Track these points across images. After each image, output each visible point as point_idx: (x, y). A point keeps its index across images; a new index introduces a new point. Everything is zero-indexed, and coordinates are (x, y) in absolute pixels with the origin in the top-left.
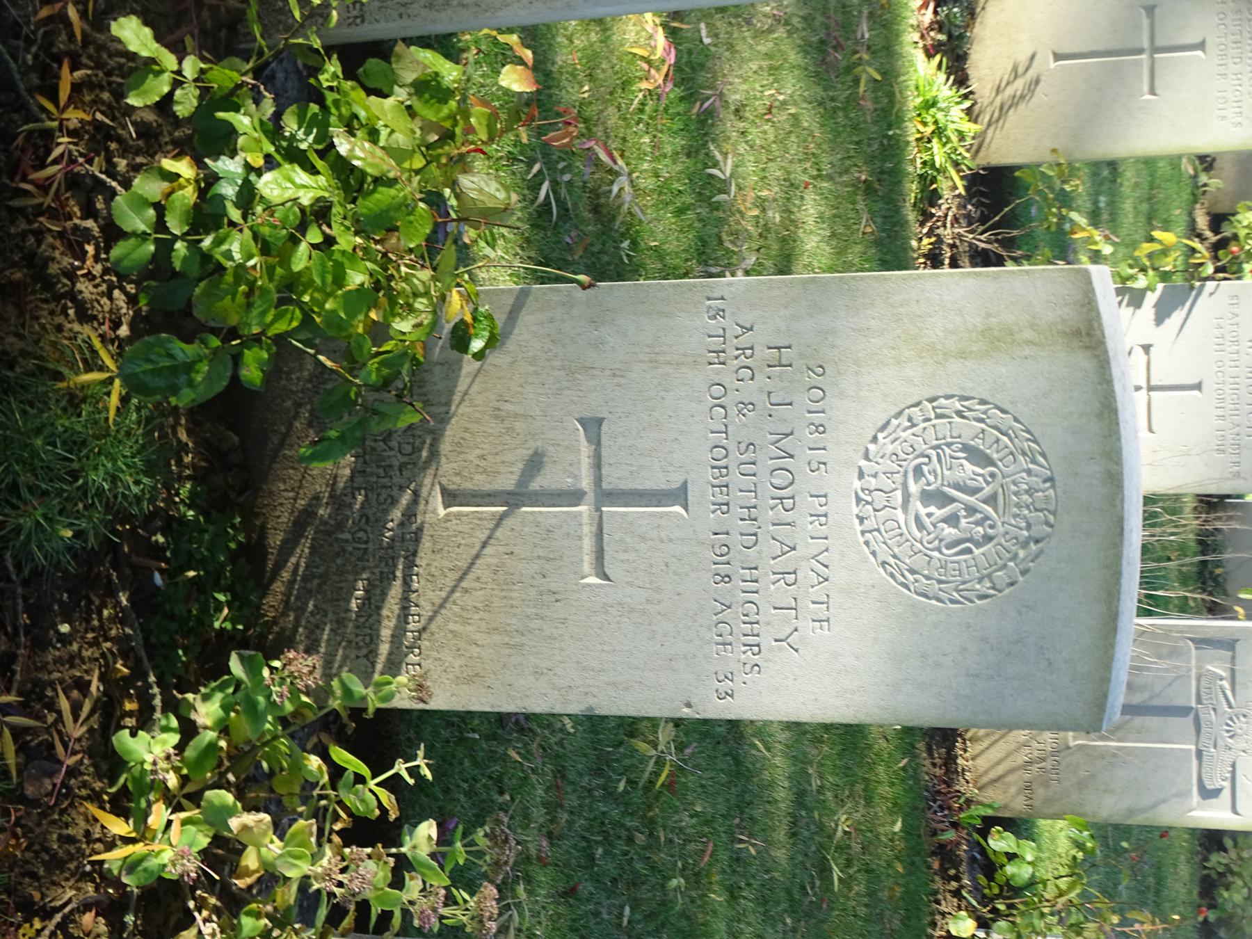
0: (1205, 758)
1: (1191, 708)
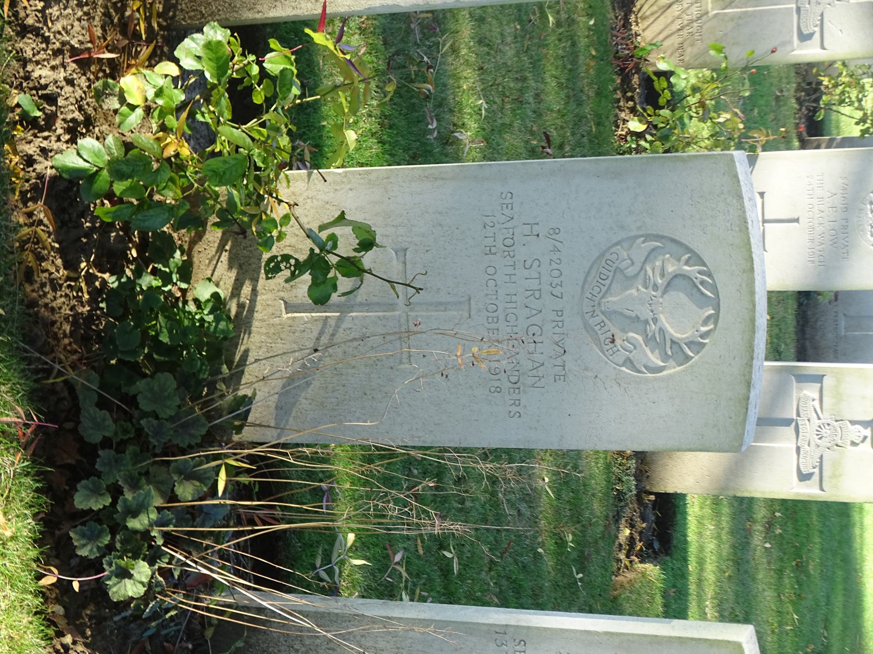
0: (802, 452)
1: (793, 420)
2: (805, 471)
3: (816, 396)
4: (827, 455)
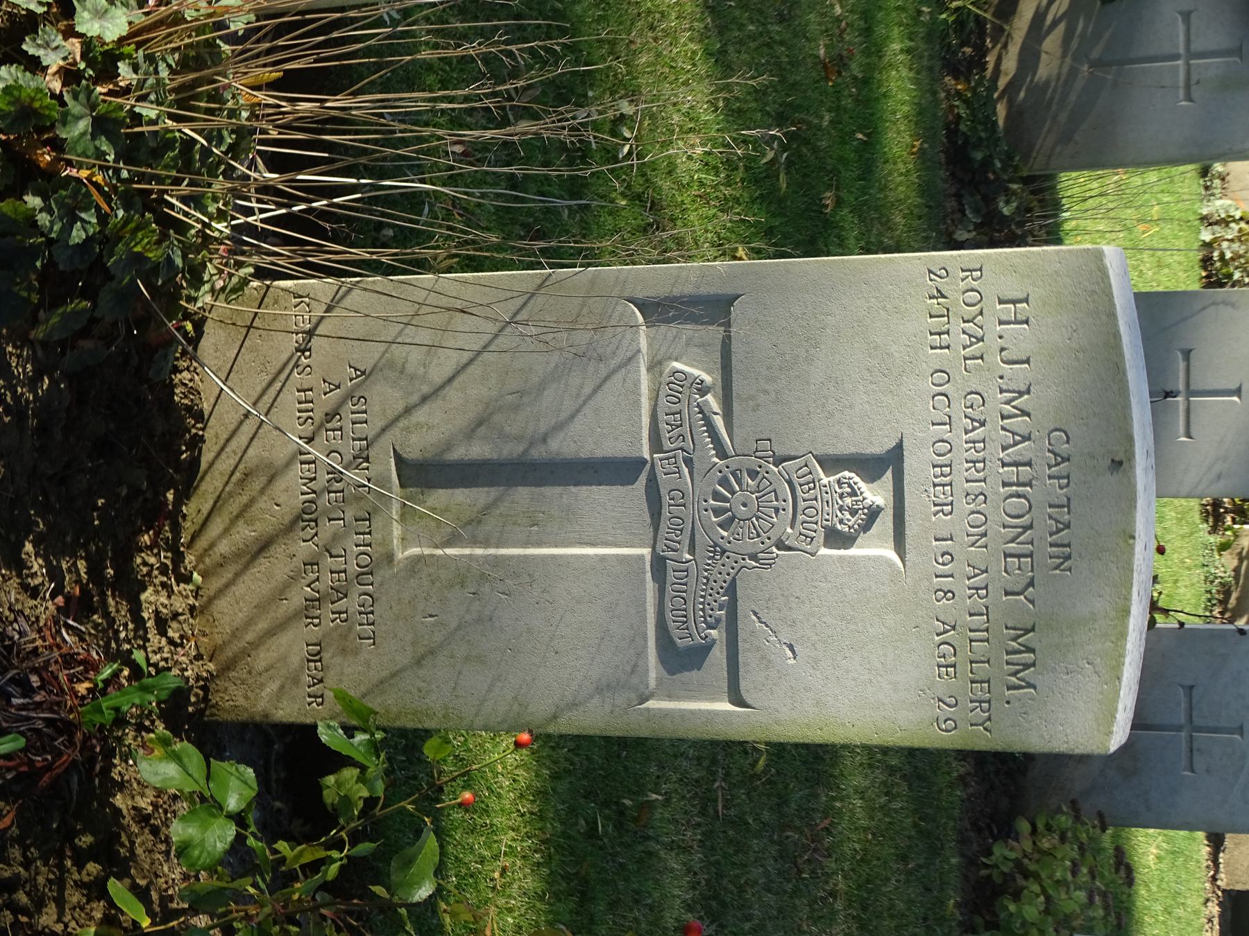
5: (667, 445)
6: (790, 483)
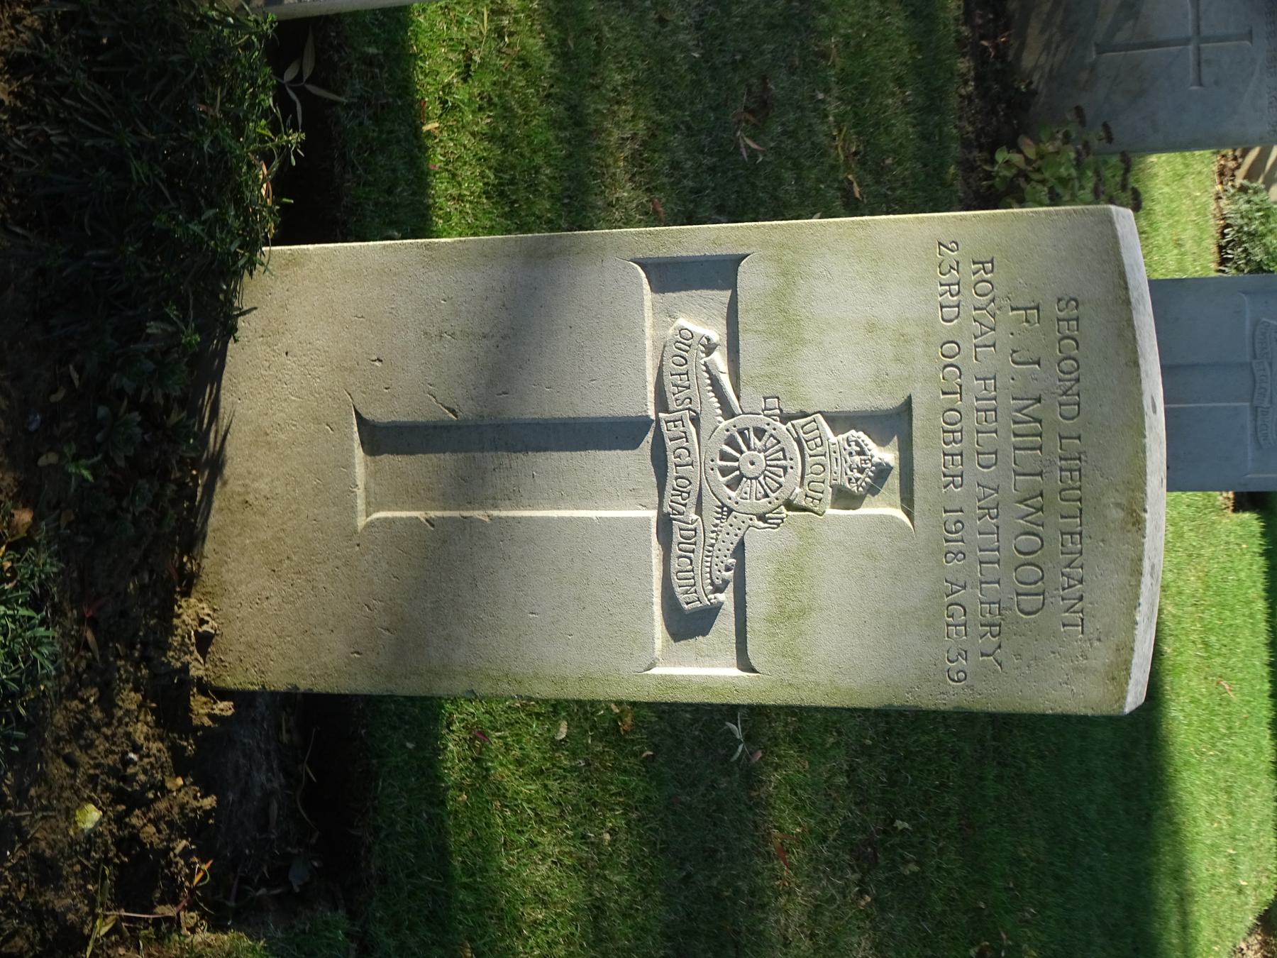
2: (688, 601)
3: (716, 333)
4: (761, 541)
5: (672, 405)
6: (798, 441)
